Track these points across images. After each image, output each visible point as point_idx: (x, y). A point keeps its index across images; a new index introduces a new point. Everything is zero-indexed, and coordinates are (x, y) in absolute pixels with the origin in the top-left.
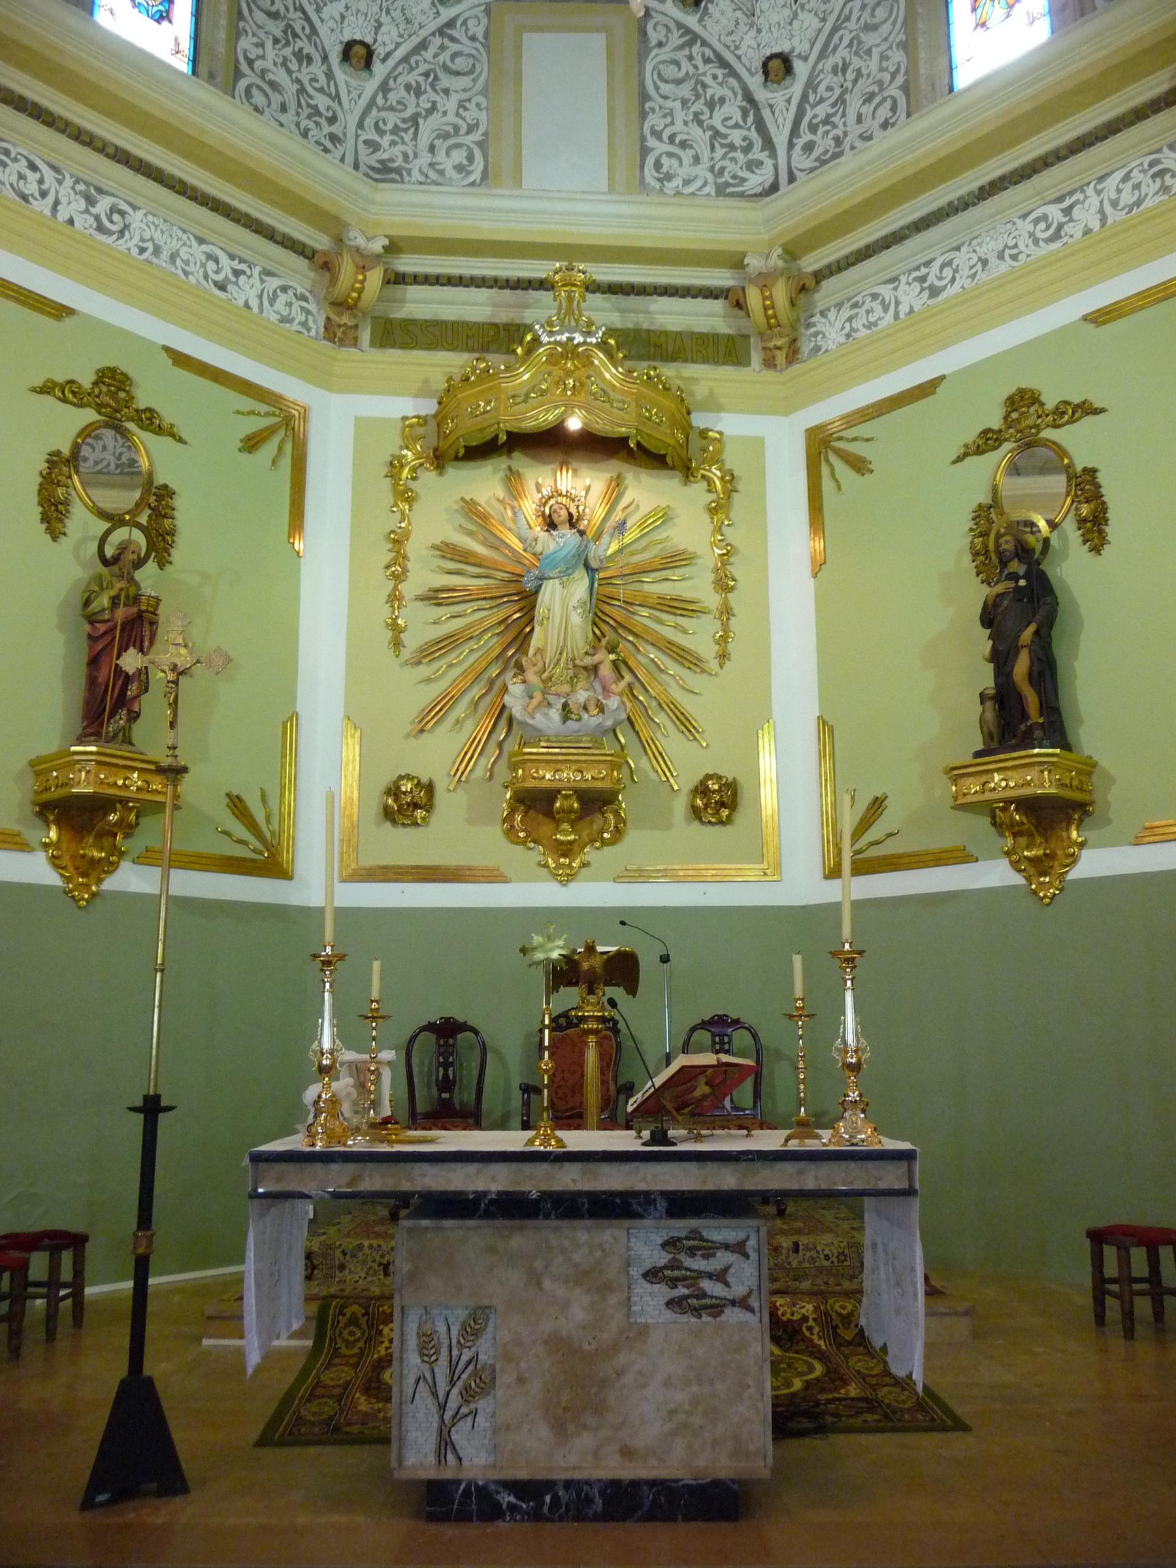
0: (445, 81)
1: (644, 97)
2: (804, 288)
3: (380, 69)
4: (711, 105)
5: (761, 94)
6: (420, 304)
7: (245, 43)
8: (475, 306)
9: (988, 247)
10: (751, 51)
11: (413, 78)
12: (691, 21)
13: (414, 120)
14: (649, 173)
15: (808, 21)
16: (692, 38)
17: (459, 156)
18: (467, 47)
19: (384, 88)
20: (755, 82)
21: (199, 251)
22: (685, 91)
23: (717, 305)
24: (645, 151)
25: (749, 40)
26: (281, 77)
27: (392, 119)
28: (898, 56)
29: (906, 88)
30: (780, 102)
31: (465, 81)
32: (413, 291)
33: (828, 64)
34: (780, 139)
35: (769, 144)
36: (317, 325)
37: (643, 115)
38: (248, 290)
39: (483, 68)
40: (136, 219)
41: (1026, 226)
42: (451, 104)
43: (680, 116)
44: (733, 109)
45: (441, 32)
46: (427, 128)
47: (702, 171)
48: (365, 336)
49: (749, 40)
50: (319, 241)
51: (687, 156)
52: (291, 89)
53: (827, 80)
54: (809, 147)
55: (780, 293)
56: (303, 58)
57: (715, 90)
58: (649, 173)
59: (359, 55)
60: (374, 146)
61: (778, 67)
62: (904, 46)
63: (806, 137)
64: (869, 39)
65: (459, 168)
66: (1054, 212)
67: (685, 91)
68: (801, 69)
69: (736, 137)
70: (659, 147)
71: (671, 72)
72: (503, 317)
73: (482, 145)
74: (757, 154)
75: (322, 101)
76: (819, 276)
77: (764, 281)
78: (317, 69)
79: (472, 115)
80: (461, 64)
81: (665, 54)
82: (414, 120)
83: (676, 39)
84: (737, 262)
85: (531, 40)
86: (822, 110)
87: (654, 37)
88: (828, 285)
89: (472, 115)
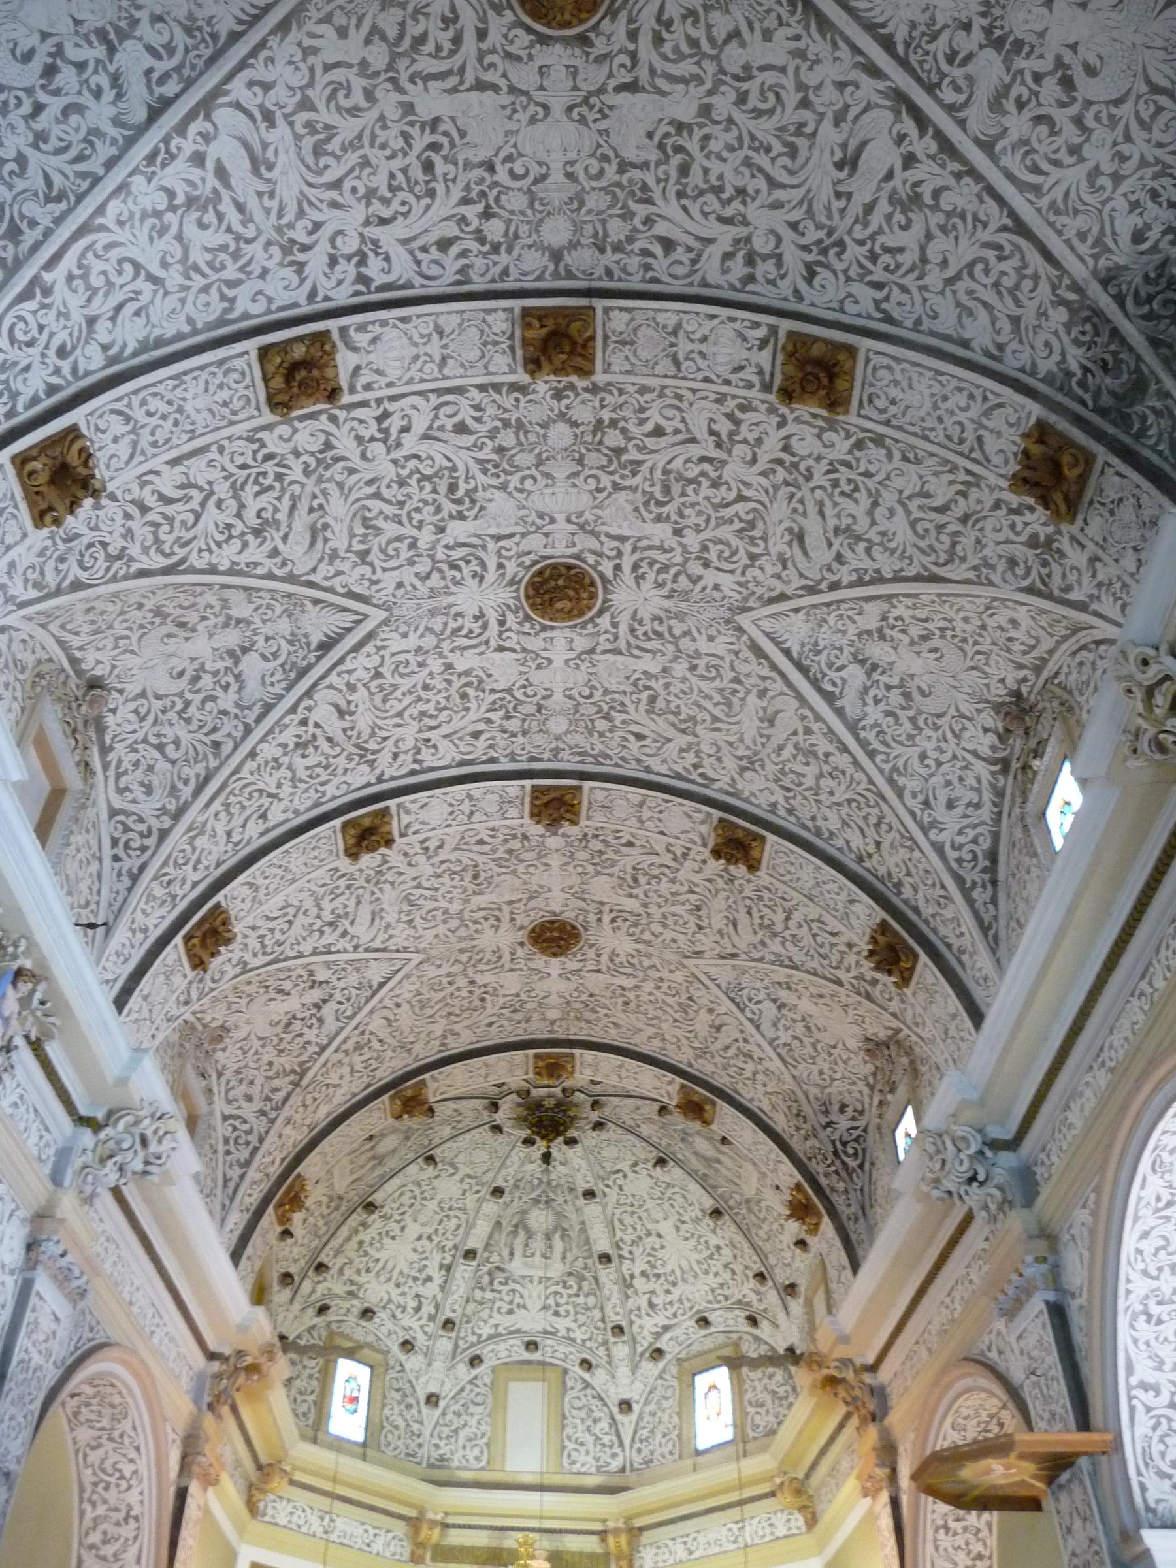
0: (472, 1409)
1: (564, 1417)
2: (635, 1533)
3: (442, 1404)
4: (595, 1421)
5: (618, 1417)
6: (456, 1538)
7: (387, 1411)
8: (480, 1539)
9: (711, 1537)
10: (614, 1395)
11: (457, 1407)
12: (586, 1376)
13: (456, 1431)
14: (566, 1461)
15: (639, 1386)
16: (587, 1385)
17: (476, 1451)
18: (483, 1390)
19: (444, 1414)
20: (615, 1410)
21: (361, 1529)
22: (583, 1414)
23: (595, 1538)
24: (563, 1448)
25: (612, 1389)
26: (400, 1422)
27: (446, 1431)
28: (676, 1419)
29: (679, 1436)
30: (627, 1422)
31: (480, 1409)
32: (452, 1531)
33: (648, 1409)
34: (627, 1441)
35: (621, 1445)
36: (406, 1555)
37: (563, 1427)
38: (378, 1546)
39: (490, 1401)
40: (339, 1522)
41: (724, 1531)
42: (473, 1422)
43: (581, 1427)
44: (604, 1424)
45: (471, 1382)
46: (463, 1434)
47: (590, 1459)
48: (428, 1555)
49: (612, 1389)
50: (413, 1513)
51: (582, 1450)
52: (402, 1424)
53: (647, 1418)
54: (639, 1451)
55: (623, 1540)
56: (409, 1407)
57: (597, 1414)
58: (566, 1461)
59: (432, 1399)
60: (437, 1446)
61: (626, 1406)
62: (679, 1414)
63: (637, 1445)
64: (665, 1404)
65: (477, 1458)
66: (735, 1527)
67: (583, 1414)
68: (636, 1408)
69: (606, 1440)
70: (570, 1445)
71: (577, 1403)
72: (494, 1544)
73: (488, 1445)
74: (616, 1450)
75: (415, 1427)
76: (641, 1529)
77: (617, 1532)
78: (414, 1411)
79: (483, 1428)
80: (480, 1399)
81: (574, 1393)
82: (456, 1431)
83: (579, 1386)
84: (604, 1521)
85: (513, 1386)
86: (645, 1433)
87: (570, 1384)
88: (646, 1534)
89: (483, 1428)
